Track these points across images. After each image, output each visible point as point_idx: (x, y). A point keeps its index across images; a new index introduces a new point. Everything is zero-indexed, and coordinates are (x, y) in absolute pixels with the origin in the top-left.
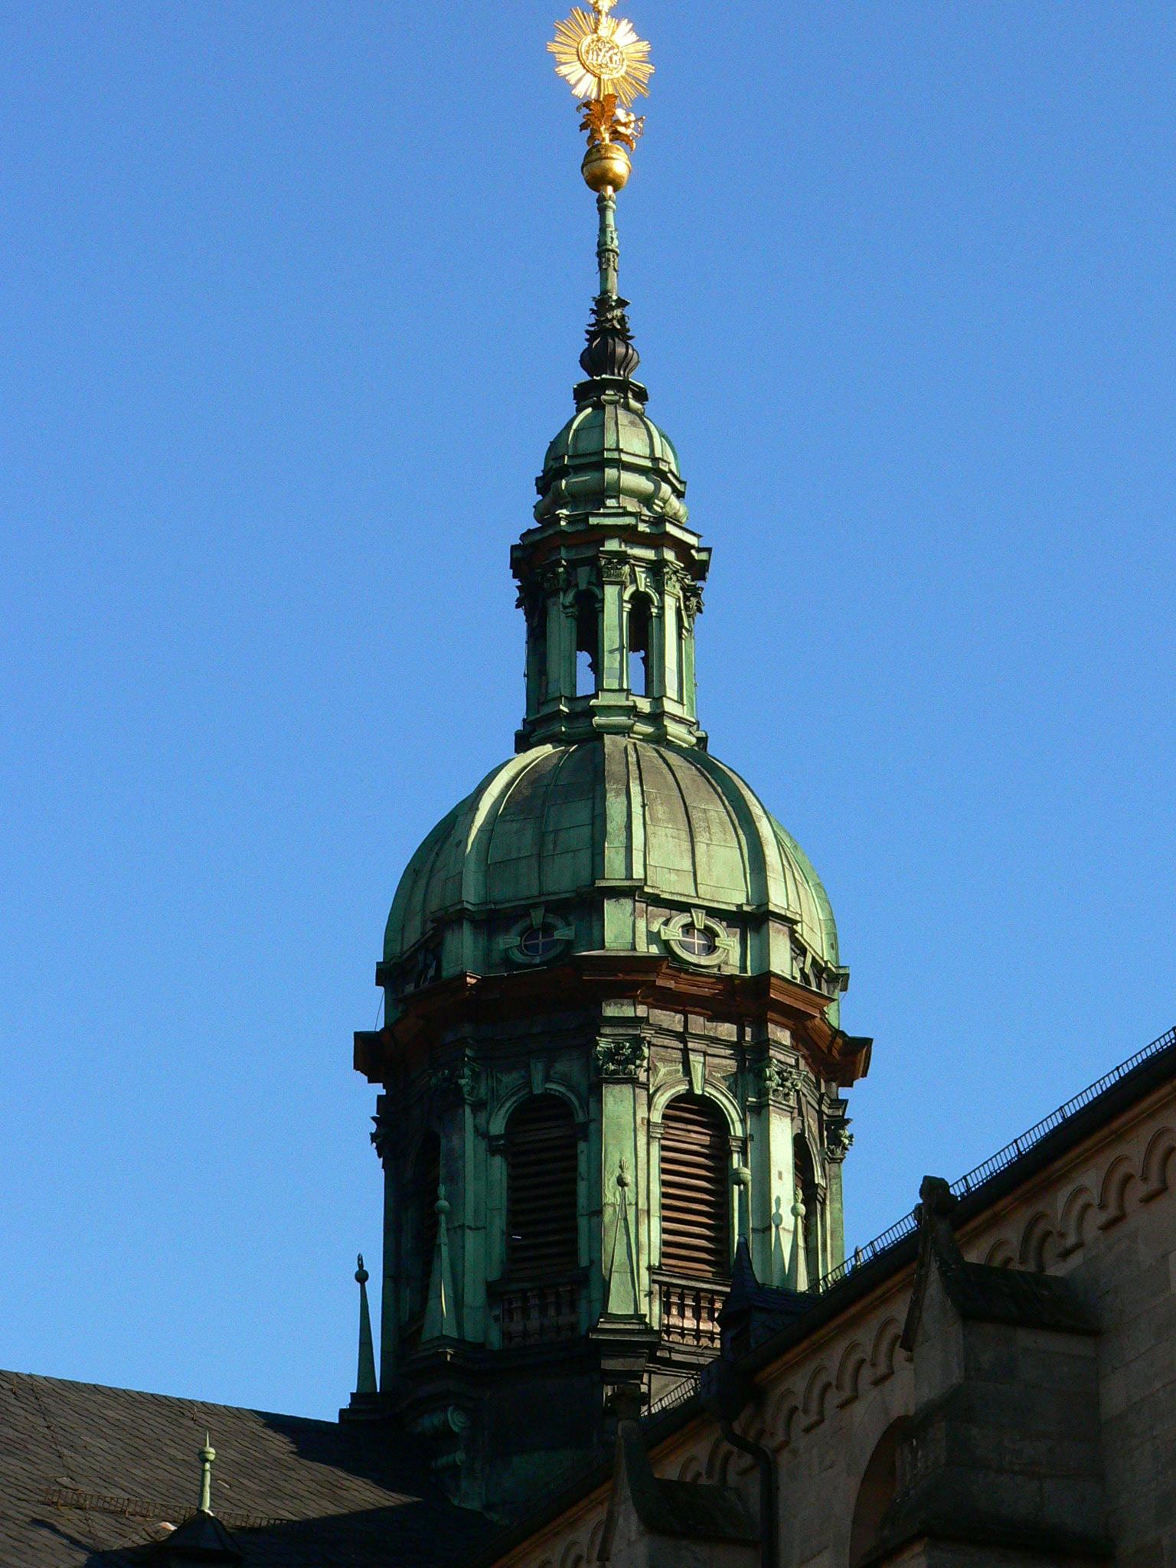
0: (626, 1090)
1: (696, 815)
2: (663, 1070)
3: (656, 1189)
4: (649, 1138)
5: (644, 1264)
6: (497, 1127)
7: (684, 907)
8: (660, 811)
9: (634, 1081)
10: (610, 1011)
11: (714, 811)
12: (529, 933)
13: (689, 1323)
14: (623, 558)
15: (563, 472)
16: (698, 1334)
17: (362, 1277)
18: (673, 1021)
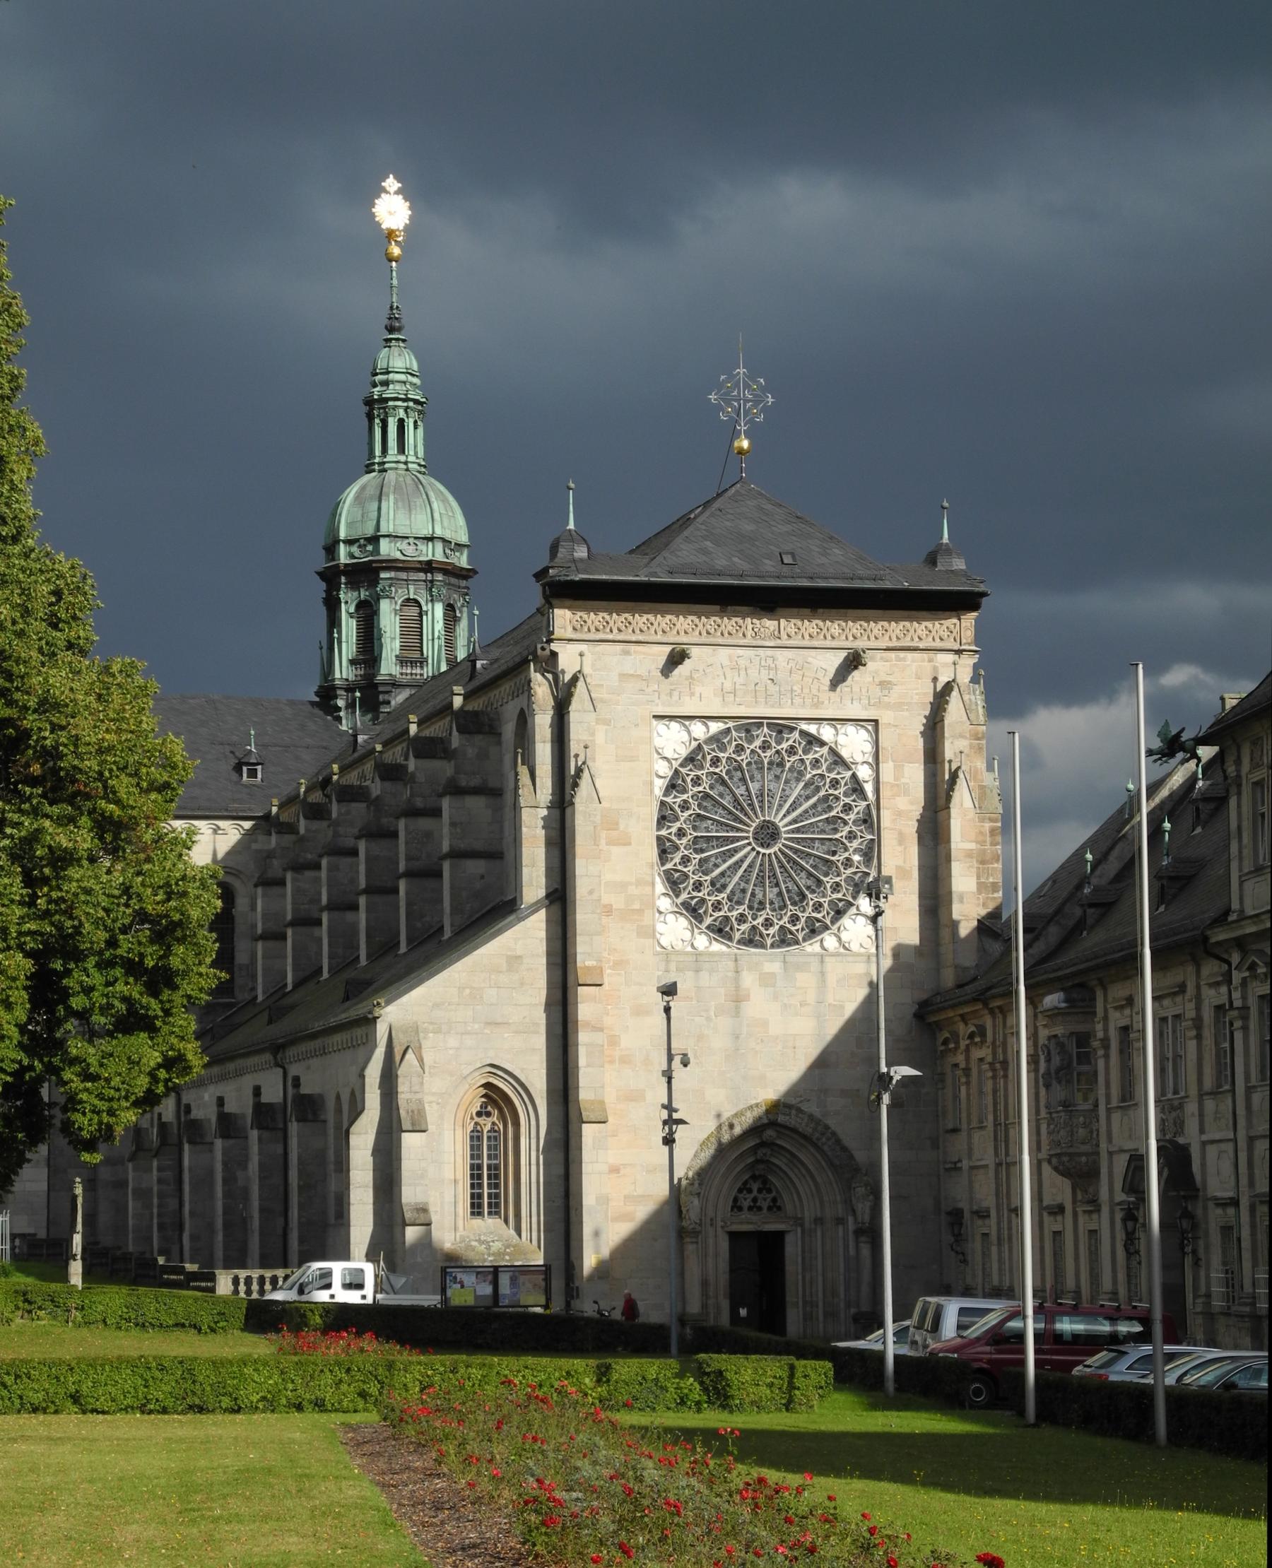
0: (387, 601)
1: (412, 504)
2: (400, 591)
3: (398, 630)
4: (396, 614)
5: (394, 654)
6: (352, 609)
7: (407, 538)
8: (400, 504)
9: (388, 597)
10: (383, 575)
11: (419, 501)
12: (360, 547)
13: (409, 671)
14: (395, 408)
15: (376, 374)
16: (412, 674)
17: (321, 648)
18: (403, 575)
